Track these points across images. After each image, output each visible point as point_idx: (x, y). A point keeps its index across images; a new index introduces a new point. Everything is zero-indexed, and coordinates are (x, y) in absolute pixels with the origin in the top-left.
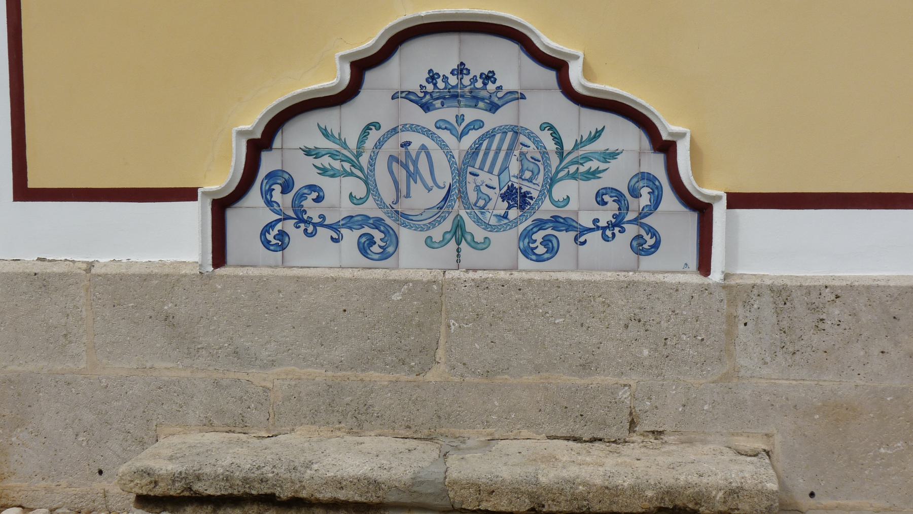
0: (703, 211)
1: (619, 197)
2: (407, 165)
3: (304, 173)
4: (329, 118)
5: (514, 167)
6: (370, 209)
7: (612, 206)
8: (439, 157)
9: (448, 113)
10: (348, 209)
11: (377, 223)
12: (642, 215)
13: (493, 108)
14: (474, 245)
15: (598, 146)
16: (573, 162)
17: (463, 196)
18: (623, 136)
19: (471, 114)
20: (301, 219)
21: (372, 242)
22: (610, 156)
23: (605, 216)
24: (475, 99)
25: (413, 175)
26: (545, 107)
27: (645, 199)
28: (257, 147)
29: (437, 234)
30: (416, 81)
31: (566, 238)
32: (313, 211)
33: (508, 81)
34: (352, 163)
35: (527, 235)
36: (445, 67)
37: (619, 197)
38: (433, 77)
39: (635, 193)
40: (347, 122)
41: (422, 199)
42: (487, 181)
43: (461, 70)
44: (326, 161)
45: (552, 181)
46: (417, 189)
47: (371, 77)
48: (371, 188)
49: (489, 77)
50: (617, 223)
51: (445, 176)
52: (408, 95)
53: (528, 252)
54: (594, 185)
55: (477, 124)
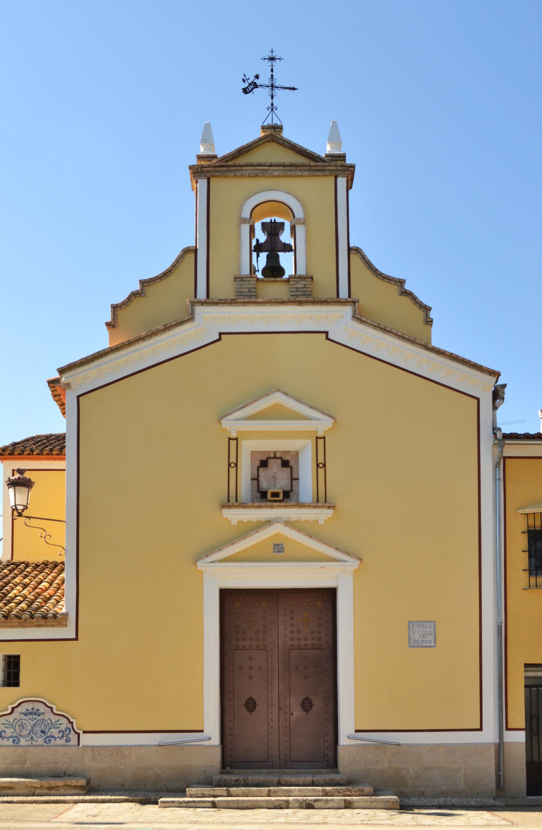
1: (63, 732)
2: (22, 726)
4: (7, 717)
5: (43, 726)
6: (15, 734)
7: (61, 733)
8: (28, 725)
9: (30, 717)
10: (10, 734)
11: (16, 737)
12: (67, 735)
13: (39, 715)
14: (35, 741)
15: (59, 722)
16: (54, 725)
17: (33, 732)
19: (34, 717)
21: (15, 740)
23: (60, 735)
24: (35, 714)
25: (23, 728)
26: (49, 715)
27: (68, 732)
29: (28, 739)
30: (24, 711)
31: (53, 739)
33: (42, 711)
35: (45, 739)
36: (30, 708)
37: (63, 732)
38: (27, 710)
39: (66, 731)
40: (11, 718)
41: (25, 732)
42: (38, 729)
43: (33, 709)
44: (6, 726)
46: (24, 730)
47: (15, 710)
48: (15, 729)
49: (38, 710)
50: (63, 736)
51: (29, 728)
52: (23, 713)
53: (45, 742)
54: (58, 730)
55: (36, 719)
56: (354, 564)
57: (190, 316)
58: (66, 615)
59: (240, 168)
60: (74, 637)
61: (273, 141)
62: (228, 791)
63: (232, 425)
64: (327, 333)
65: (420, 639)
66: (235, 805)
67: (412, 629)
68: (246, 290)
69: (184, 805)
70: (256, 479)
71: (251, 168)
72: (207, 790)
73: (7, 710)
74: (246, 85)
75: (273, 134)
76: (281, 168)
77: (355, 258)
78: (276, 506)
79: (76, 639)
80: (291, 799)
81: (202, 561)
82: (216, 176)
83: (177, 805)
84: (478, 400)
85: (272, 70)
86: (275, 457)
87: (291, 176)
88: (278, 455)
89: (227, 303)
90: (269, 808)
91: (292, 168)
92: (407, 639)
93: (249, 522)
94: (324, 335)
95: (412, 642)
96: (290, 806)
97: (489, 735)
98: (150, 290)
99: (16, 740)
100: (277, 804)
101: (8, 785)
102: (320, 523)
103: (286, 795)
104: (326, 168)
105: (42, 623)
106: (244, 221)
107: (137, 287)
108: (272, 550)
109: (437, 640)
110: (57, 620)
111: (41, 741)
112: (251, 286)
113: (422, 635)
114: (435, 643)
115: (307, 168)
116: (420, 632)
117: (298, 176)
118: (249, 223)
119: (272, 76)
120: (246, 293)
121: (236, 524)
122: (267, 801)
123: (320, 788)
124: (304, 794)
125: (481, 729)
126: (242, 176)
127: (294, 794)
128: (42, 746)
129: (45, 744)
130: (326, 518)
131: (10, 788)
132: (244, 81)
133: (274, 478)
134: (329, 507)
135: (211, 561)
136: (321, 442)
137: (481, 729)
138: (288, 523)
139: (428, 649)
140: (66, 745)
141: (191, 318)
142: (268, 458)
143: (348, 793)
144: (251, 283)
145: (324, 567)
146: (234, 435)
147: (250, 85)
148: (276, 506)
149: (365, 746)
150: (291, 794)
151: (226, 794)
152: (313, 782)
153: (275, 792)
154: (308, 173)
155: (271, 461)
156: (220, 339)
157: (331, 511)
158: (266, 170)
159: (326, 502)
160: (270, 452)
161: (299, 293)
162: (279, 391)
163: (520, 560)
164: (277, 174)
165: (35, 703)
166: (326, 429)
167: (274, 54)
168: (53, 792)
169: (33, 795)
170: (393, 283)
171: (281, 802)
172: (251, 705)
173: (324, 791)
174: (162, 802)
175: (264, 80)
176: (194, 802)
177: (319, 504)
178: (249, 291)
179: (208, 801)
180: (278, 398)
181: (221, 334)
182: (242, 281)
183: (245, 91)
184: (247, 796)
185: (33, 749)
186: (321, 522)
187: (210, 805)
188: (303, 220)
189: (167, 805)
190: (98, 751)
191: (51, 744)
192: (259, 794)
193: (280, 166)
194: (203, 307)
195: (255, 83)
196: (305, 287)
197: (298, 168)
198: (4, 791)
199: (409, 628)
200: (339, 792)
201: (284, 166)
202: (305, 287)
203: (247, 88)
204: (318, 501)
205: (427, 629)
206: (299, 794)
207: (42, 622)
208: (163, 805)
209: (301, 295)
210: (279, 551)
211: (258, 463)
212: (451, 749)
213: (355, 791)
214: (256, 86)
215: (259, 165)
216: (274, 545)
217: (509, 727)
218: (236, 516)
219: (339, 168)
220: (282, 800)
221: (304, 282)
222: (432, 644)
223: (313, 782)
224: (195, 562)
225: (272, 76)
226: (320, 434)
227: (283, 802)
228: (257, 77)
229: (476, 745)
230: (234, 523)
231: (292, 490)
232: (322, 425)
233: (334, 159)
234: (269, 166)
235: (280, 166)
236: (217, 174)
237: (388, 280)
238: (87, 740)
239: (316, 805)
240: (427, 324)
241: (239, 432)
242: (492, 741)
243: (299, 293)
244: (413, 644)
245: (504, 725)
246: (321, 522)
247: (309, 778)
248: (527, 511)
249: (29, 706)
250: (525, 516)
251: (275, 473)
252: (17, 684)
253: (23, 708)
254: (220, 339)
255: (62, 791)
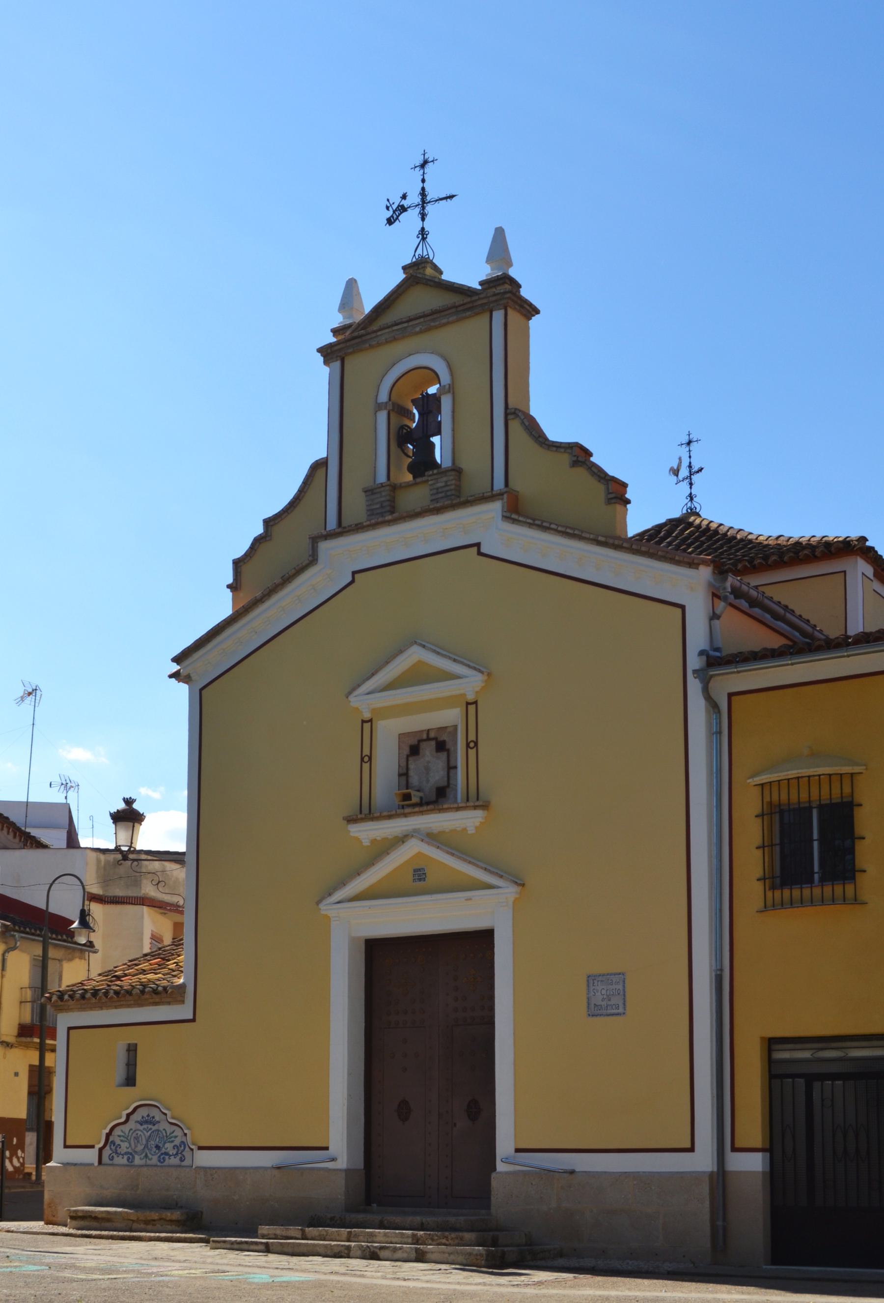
0: (192, 1150)
3: (118, 1142)
4: (122, 1127)
6: (130, 1150)
9: (145, 1126)
10: (125, 1150)
11: (131, 1154)
18: (178, 1133)
19: (150, 1126)
20: (116, 1153)
22: (176, 1137)
28: (108, 1135)
30: (139, 1119)
31: (167, 1157)
32: (119, 1151)
33: (157, 1119)
34: (126, 1138)
40: (126, 1128)
41: (140, 1148)
43: (148, 1116)
45: (165, 1143)
48: (130, 1145)
49: (153, 1117)
50: (177, 1154)
51: (144, 1142)
54: (172, 1144)
56: (510, 892)
57: (311, 558)
58: (183, 987)
59: (373, 335)
60: (191, 1017)
61: (417, 283)
62: (303, 1231)
63: (363, 702)
64: (478, 545)
65: (604, 1003)
66: (290, 1250)
67: (592, 988)
68: (378, 506)
69: (236, 1246)
70: (404, 774)
71: (387, 331)
72: (278, 1230)
73: (121, 1118)
74: (389, 214)
75: (420, 273)
76: (422, 320)
77: (515, 425)
78: (410, 813)
79: (193, 1020)
80: (353, 1244)
81: (325, 902)
82: (351, 353)
83: (228, 1246)
84: (683, 608)
85: (423, 181)
86: (428, 739)
87: (436, 327)
88: (432, 735)
89: (353, 530)
90: (324, 1256)
91: (435, 316)
92: (585, 1004)
93: (385, 839)
94: (475, 549)
95: (592, 1006)
96: (351, 1254)
97: (702, 1160)
98: (276, 530)
99: (130, 1156)
100: (336, 1250)
101: (104, 1215)
102: (469, 832)
103: (370, 1240)
104: (475, 304)
105: (157, 1000)
106: (379, 407)
107: (259, 530)
108: (411, 877)
109: (627, 1004)
110: (174, 995)
111: (154, 1160)
112: (382, 499)
113: (606, 996)
114: (625, 1008)
115: (454, 310)
116: (604, 992)
117: (445, 325)
118: (386, 408)
119: (423, 189)
120: (385, 508)
121: (368, 844)
122: (325, 1246)
123: (410, 1232)
124: (389, 1240)
125: (692, 1149)
126: (379, 345)
127: (378, 1239)
128: (156, 1166)
129: (159, 1164)
130: (478, 824)
131: (108, 1220)
132: (388, 208)
133: (427, 769)
134: (475, 807)
135: (339, 899)
136: (472, 708)
137: (692, 1149)
138: (433, 838)
139: (614, 1018)
140: (180, 1166)
141: (313, 559)
142: (419, 741)
143: (444, 1241)
144: (383, 494)
145: (470, 899)
146: (367, 716)
147: (394, 212)
148: (410, 813)
149: (525, 1173)
150: (375, 1239)
151: (300, 1236)
152: (422, 1224)
153: (356, 1236)
154: (454, 318)
155: (423, 745)
156: (353, 581)
157: (479, 813)
158: (405, 328)
159: (478, 799)
160: (422, 731)
161: (440, 495)
162: (416, 643)
163: (752, 863)
164: (418, 329)
165: (151, 1108)
166: (477, 689)
167: (426, 156)
168: (150, 1227)
169: (131, 1231)
170: (563, 450)
171: (343, 1248)
172: (404, 1110)
173: (414, 1236)
174: (213, 1241)
175: (414, 198)
176: (246, 1242)
177: (468, 804)
178: (382, 507)
179: (262, 1243)
180: (415, 655)
181: (354, 573)
182: (373, 494)
183: (390, 222)
184: (324, 1240)
185: (145, 1169)
186: (471, 830)
187: (262, 1247)
188: (447, 387)
189: (219, 1245)
190: (211, 1175)
191: (165, 1164)
192: (338, 1238)
193: (420, 317)
194: (327, 541)
195: (402, 206)
196: (447, 486)
197: (443, 314)
198: (103, 1224)
199: (588, 986)
200: (433, 1240)
201: (424, 316)
202: (447, 486)
203: (392, 216)
204: (468, 800)
205: (614, 987)
206: (383, 1239)
207: (157, 999)
208: (214, 1245)
209: (442, 498)
210: (419, 881)
211: (406, 751)
212: (642, 1180)
213: (452, 1239)
214: (402, 209)
215: (396, 324)
216: (415, 871)
217: (738, 1144)
218: (367, 832)
219: (492, 299)
220: (342, 1246)
221: (445, 479)
222: (621, 1010)
223: (422, 1224)
224: (318, 903)
225: (423, 189)
226: (471, 697)
227: (343, 1248)
228: (404, 197)
229: (681, 1175)
230: (366, 843)
231: (448, 785)
232: (471, 684)
233: (492, 285)
234: (408, 322)
235: (420, 317)
236: (350, 351)
237: (555, 449)
238: (205, 1159)
239: (382, 1254)
240: (610, 504)
241: (373, 711)
242: (710, 1169)
243: (440, 495)
244: (594, 1011)
245: (726, 1141)
246: (471, 830)
247: (418, 1219)
248: (764, 778)
249: (143, 1112)
250: (760, 788)
251: (428, 762)
252: (134, 1085)
253: (135, 1117)
254: (353, 581)
255: (158, 1226)
